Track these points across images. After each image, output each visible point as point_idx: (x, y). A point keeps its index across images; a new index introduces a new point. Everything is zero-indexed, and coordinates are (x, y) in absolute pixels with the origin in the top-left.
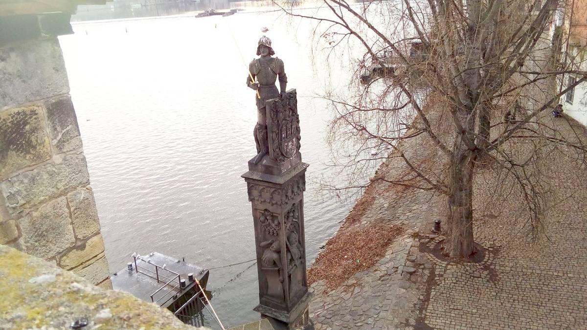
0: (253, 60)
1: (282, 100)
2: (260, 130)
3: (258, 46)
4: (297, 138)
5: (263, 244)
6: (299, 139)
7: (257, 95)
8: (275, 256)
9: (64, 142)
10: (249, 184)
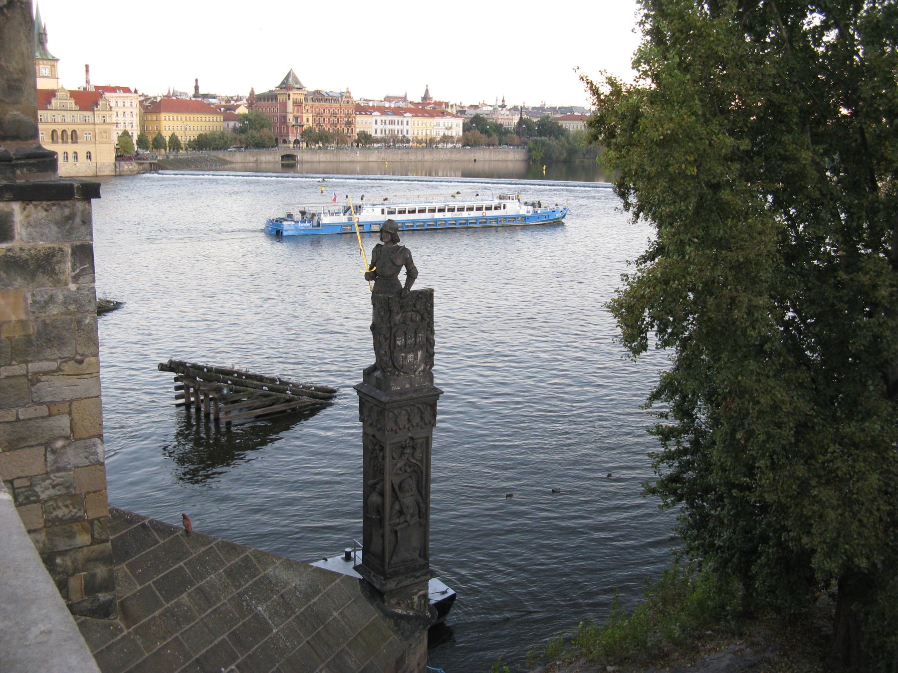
4: (427, 352)
5: (371, 482)
8: (379, 500)
10: (361, 398)
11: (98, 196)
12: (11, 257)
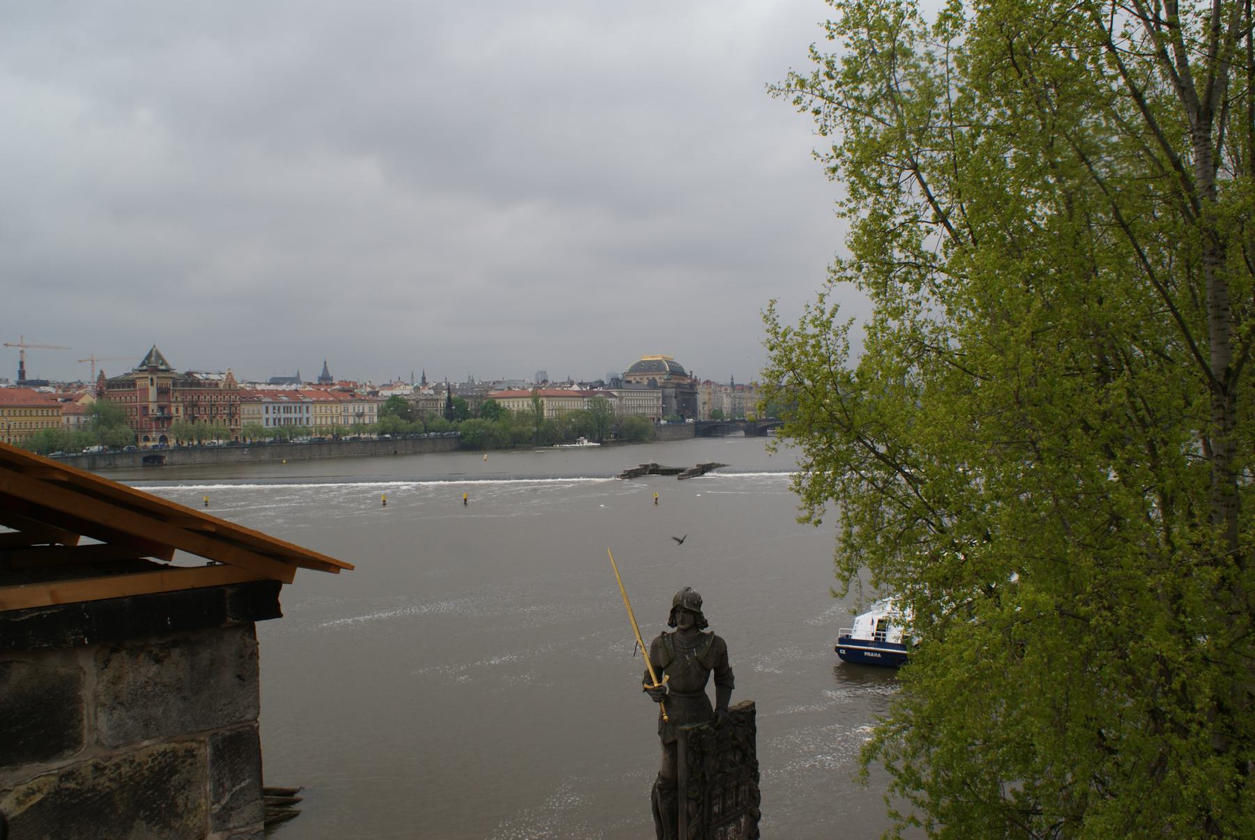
0: (660, 634)
1: (717, 728)
2: (664, 792)
3: (672, 607)
4: (751, 815)
6: (755, 818)
7: (662, 713)
9: (232, 809)
11: (273, 611)
12: (72, 793)
